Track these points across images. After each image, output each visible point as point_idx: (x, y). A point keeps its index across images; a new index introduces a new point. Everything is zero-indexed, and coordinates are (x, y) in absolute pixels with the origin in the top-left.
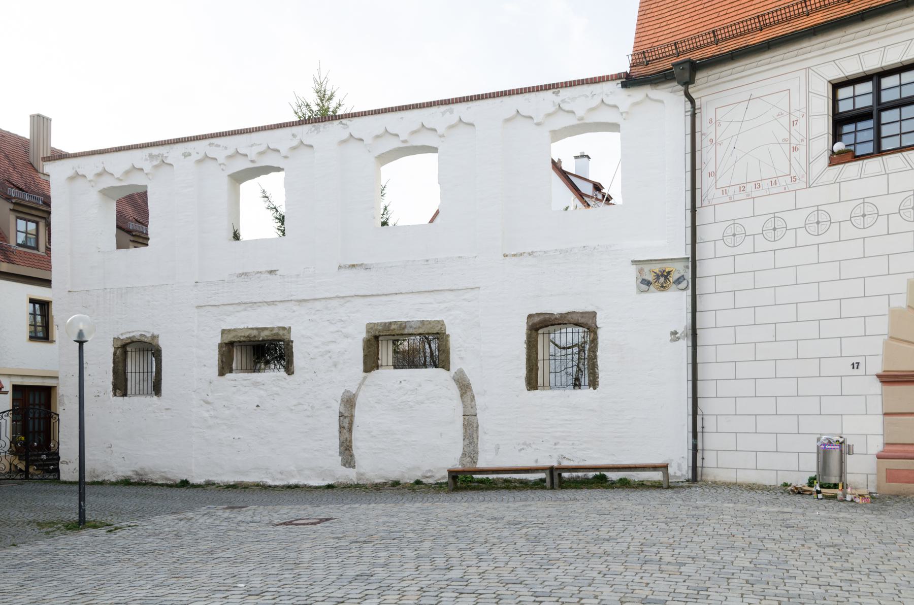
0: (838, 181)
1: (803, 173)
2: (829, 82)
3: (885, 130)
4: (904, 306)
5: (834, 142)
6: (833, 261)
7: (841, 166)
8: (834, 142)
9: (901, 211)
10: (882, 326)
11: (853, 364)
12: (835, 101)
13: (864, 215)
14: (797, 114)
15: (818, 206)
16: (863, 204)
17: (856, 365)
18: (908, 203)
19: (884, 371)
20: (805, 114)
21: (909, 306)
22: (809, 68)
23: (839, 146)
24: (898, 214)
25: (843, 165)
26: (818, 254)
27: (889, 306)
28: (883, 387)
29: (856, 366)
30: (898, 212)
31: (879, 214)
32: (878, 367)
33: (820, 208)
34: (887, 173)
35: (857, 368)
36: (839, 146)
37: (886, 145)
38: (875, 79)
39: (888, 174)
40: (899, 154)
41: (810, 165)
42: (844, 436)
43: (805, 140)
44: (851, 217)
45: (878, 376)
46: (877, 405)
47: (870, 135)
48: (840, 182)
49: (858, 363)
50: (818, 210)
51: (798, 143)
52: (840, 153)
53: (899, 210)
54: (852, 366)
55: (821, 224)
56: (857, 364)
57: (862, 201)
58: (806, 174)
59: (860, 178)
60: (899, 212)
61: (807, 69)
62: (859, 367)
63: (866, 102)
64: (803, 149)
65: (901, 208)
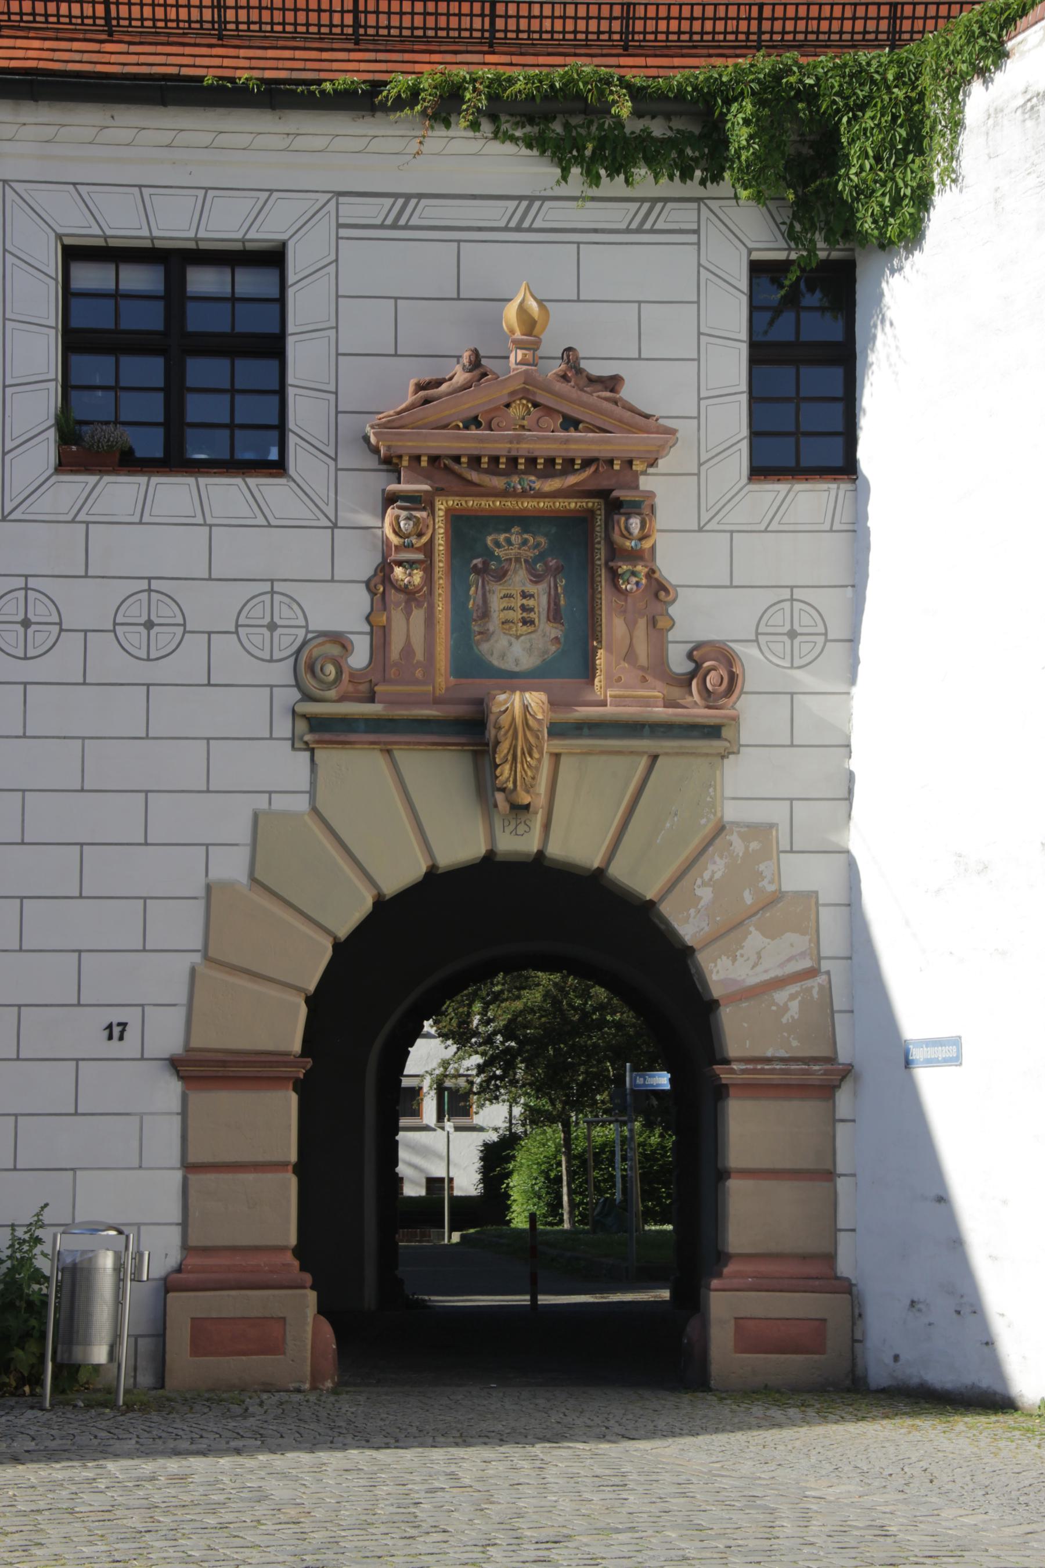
0: (82, 517)
2: (59, 237)
6: (65, 738)
9: (240, 629)
11: (110, 1027)
13: (149, 625)
15: (26, 577)
16: (146, 594)
17: (115, 1031)
18: (258, 612)
24: (235, 636)
27: (207, 875)
29: (116, 1031)
30: (233, 630)
33: (32, 583)
34: (208, 522)
35: (121, 1038)
39: (211, 526)
44: (115, 624)
47: (154, 407)
48: (87, 523)
49: (123, 1025)
50: (26, 589)
53: (237, 626)
54: (107, 1032)
55: (33, 628)
56: (120, 1028)
59: (140, 523)
60: (237, 632)
62: (126, 1034)
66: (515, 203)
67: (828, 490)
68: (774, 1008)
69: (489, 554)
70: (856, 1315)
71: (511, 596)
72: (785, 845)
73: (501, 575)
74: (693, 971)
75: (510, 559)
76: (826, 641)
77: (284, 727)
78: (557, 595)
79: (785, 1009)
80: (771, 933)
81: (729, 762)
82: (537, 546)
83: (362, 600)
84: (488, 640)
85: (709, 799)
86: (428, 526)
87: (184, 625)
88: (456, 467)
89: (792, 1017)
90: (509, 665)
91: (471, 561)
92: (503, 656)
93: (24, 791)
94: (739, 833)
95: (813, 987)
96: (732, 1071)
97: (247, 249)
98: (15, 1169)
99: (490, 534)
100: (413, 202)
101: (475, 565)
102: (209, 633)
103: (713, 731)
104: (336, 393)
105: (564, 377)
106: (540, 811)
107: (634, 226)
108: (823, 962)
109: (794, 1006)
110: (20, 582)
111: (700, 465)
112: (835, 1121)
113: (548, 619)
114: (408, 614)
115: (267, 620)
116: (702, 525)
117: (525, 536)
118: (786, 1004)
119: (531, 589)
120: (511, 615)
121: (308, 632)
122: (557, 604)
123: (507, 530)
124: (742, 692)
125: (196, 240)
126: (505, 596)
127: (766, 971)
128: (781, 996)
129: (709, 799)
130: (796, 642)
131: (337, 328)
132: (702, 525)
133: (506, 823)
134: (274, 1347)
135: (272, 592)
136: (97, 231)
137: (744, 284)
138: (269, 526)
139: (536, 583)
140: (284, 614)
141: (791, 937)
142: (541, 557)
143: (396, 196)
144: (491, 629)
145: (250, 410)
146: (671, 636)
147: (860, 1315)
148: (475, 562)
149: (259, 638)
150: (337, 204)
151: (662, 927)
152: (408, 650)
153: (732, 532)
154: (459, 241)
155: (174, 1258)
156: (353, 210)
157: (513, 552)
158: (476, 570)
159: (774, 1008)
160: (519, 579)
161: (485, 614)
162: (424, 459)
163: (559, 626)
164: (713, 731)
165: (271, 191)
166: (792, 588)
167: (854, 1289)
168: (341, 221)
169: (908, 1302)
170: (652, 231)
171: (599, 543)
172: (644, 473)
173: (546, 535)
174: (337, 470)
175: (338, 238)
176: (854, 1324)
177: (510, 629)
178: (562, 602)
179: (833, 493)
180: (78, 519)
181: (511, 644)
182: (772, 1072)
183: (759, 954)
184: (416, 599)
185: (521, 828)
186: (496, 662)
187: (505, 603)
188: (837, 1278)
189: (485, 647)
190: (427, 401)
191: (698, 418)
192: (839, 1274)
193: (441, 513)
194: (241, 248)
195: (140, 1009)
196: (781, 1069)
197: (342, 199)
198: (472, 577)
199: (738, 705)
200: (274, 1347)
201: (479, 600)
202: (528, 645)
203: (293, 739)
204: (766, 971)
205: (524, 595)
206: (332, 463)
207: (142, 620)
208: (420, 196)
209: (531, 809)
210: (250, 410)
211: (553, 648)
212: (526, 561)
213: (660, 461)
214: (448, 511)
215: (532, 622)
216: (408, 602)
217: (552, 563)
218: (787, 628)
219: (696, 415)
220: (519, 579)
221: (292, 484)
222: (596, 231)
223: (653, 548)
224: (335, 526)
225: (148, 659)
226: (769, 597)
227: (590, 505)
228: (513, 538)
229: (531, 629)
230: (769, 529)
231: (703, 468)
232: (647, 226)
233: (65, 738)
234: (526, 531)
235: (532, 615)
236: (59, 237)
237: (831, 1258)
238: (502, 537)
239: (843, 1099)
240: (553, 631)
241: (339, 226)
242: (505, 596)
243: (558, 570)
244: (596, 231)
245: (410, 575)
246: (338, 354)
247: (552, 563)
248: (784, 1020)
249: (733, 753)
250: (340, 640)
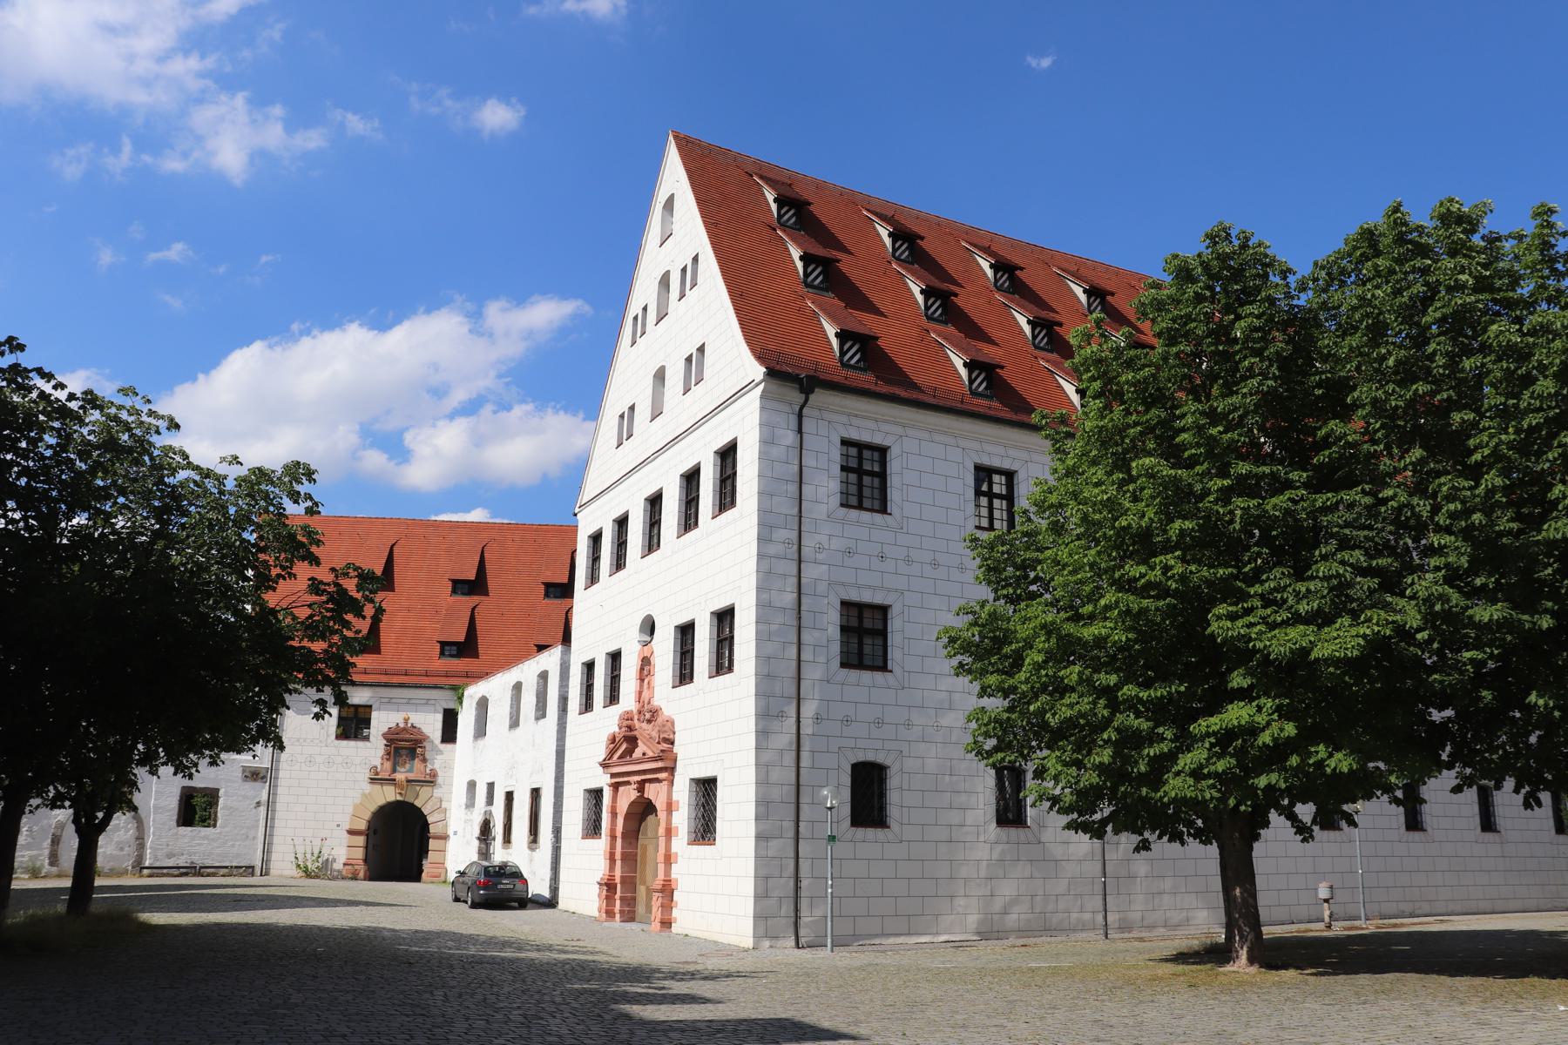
10: (350, 810)
17: (338, 826)
32: (347, 827)
46: (345, 843)
103: (432, 782)
156: (383, 700)
164: (432, 782)
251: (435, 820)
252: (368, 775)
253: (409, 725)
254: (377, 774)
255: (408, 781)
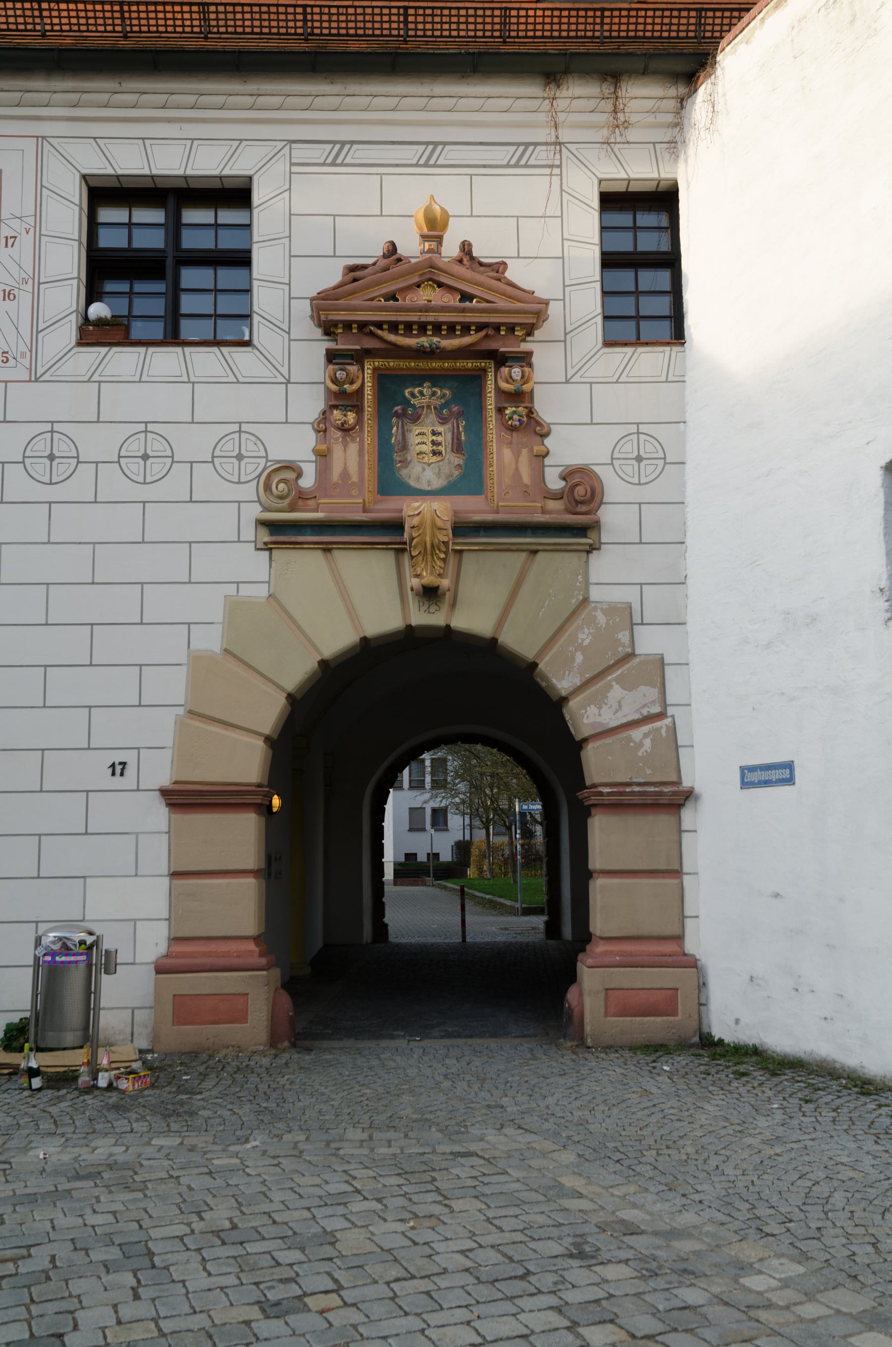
1: (23, 348)
2: (84, 177)
3: (188, 304)
4: (217, 649)
5: (89, 301)
6: (80, 543)
7: (104, 350)
8: (89, 301)
11: (113, 765)
12: (93, 226)
13: (145, 457)
14: (16, 224)
15: (52, 422)
17: (118, 769)
18: (229, 446)
19: (175, 783)
20: (32, 230)
21: (226, 650)
22: (43, 138)
23: (98, 310)
25: (107, 349)
26: (49, 524)
27: (189, 647)
28: (173, 816)
29: (118, 769)
31: (175, 460)
34: (193, 379)
35: (122, 774)
36: (98, 310)
37: (187, 328)
38: (171, 202)
39: (193, 383)
40: (215, 349)
41: (40, 335)
42: (98, 929)
43: (30, 281)
44: (119, 457)
45: (164, 792)
47: (158, 307)
48: (100, 382)
49: (124, 764)
50: (52, 432)
51: (17, 286)
52: (100, 323)
53: (213, 457)
54: (110, 770)
55: (57, 461)
56: (121, 767)
57: (142, 427)
58: (31, 351)
59: (140, 381)
60: (213, 462)
61: (40, 139)
63: (154, 240)
64: (25, 299)
65: (215, 455)
66: (424, 147)
67: (664, 352)
68: (632, 744)
69: (406, 403)
70: (702, 985)
71: (424, 434)
72: (637, 619)
73: (416, 419)
74: (567, 717)
75: (423, 407)
76: (665, 463)
77: (249, 532)
78: (459, 433)
79: (640, 745)
80: (629, 685)
81: (594, 557)
82: (443, 396)
83: (309, 439)
84: (406, 467)
85: (578, 584)
86: (358, 377)
87: (172, 457)
88: (379, 332)
89: (646, 751)
90: (424, 486)
91: (393, 408)
92: (418, 479)
93: (48, 584)
94: (602, 609)
95: (661, 727)
96: (601, 794)
97: (226, 187)
98: (39, 877)
99: (407, 388)
100: (347, 147)
101: (396, 411)
102: (192, 463)
103: (581, 530)
104: (289, 284)
105: (461, 261)
106: (448, 593)
107: (513, 162)
108: (668, 708)
109: (648, 743)
110: (48, 427)
111: (566, 334)
112: (680, 832)
113: (452, 451)
114: (345, 445)
115: (237, 452)
116: (568, 377)
117: (434, 389)
118: (641, 741)
119: (440, 429)
120: (424, 448)
121: (267, 461)
122: (459, 439)
123: (421, 385)
124: (601, 503)
125: (186, 178)
126: (420, 434)
127: (625, 716)
128: (637, 734)
129: (578, 584)
130: (642, 464)
131: (290, 237)
132: (568, 377)
133: (421, 604)
134: (240, 1017)
135: (240, 431)
136: (110, 171)
137: (596, 203)
138: (238, 382)
139: (443, 424)
140: (249, 447)
141: (643, 689)
142: (446, 405)
143: (334, 143)
144: (409, 458)
145: (227, 304)
146: (547, 461)
147: (704, 984)
148: (396, 408)
149: (230, 466)
150: (291, 149)
151: (543, 684)
152: (345, 474)
153: (591, 383)
154: (381, 175)
155: (162, 949)
156: (301, 153)
157: (425, 401)
158: (396, 414)
159: (632, 744)
160: (430, 422)
161: (404, 447)
162: (355, 326)
163: (461, 456)
164: (581, 530)
165: (241, 140)
166: (638, 424)
167: (699, 963)
168: (293, 161)
169: (748, 978)
170: (526, 166)
171: (490, 392)
172: (524, 340)
173: (449, 388)
174: (290, 340)
175: (291, 173)
176: (700, 991)
177: (423, 458)
178: (463, 438)
179: (667, 354)
180: (92, 379)
181: (424, 470)
182: (632, 793)
183: (619, 702)
184: (350, 436)
185: (432, 609)
186: (413, 483)
187: (418, 439)
188: (685, 954)
189: (404, 472)
190: (355, 280)
191: (564, 300)
192: (686, 952)
193: (369, 371)
194: (219, 186)
195: (136, 751)
196: (639, 792)
197: (294, 146)
198: (394, 420)
199: (599, 513)
200: (240, 1017)
201: (400, 438)
202: (437, 470)
203: (255, 542)
204: (625, 716)
205: (434, 433)
206: (286, 336)
207: (140, 454)
208: (352, 143)
209: (440, 591)
210: (227, 304)
211: (457, 473)
212: (435, 408)
213: (536, 332)
214: (375, 370)
215: (440, 453)
216: (344, 438)
217: (455, 409)
218: (635, 454)
219: (562, 298)
220: (430, 422)
221: (256, 351)
222: (484, 166)
223: (532, 391)
224: (288, 382)
225: (145, 483)
226: (622, 431)
227: (483, 364)
228: (425, 390)
229: (439, 458)
230: (620, 380)
231: (568, 337)
232: (523, 162)
233: (80, 543)
234: (434, 385)
235: (440, 448)
236: (84, 177)
237: (679, 938)
238: (416, 390)
239: (687, 815)
240: (457, 460)
241: (292, 164)
242: (420, 434)
243: (459, 415)
244: (484, 166)
245: (345, 415)
246: (291, 256)
247: (455, 409)
248: (640, 754)
249: (596, 549)
250: (292, 468)
251: (609, 718)
252: (254, 511)
253: (450, 249)
254: (301, 498)
255: (462, 529)
